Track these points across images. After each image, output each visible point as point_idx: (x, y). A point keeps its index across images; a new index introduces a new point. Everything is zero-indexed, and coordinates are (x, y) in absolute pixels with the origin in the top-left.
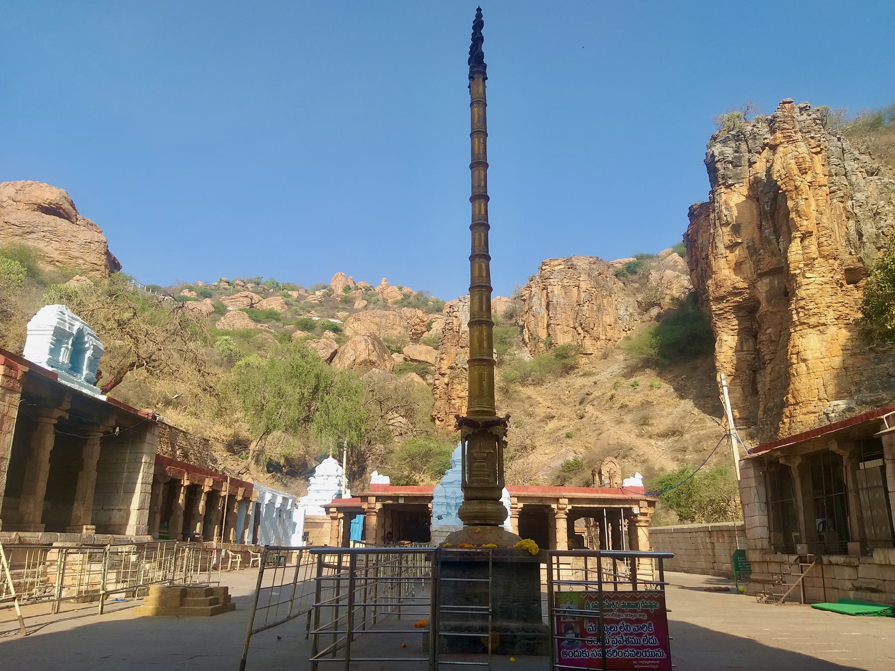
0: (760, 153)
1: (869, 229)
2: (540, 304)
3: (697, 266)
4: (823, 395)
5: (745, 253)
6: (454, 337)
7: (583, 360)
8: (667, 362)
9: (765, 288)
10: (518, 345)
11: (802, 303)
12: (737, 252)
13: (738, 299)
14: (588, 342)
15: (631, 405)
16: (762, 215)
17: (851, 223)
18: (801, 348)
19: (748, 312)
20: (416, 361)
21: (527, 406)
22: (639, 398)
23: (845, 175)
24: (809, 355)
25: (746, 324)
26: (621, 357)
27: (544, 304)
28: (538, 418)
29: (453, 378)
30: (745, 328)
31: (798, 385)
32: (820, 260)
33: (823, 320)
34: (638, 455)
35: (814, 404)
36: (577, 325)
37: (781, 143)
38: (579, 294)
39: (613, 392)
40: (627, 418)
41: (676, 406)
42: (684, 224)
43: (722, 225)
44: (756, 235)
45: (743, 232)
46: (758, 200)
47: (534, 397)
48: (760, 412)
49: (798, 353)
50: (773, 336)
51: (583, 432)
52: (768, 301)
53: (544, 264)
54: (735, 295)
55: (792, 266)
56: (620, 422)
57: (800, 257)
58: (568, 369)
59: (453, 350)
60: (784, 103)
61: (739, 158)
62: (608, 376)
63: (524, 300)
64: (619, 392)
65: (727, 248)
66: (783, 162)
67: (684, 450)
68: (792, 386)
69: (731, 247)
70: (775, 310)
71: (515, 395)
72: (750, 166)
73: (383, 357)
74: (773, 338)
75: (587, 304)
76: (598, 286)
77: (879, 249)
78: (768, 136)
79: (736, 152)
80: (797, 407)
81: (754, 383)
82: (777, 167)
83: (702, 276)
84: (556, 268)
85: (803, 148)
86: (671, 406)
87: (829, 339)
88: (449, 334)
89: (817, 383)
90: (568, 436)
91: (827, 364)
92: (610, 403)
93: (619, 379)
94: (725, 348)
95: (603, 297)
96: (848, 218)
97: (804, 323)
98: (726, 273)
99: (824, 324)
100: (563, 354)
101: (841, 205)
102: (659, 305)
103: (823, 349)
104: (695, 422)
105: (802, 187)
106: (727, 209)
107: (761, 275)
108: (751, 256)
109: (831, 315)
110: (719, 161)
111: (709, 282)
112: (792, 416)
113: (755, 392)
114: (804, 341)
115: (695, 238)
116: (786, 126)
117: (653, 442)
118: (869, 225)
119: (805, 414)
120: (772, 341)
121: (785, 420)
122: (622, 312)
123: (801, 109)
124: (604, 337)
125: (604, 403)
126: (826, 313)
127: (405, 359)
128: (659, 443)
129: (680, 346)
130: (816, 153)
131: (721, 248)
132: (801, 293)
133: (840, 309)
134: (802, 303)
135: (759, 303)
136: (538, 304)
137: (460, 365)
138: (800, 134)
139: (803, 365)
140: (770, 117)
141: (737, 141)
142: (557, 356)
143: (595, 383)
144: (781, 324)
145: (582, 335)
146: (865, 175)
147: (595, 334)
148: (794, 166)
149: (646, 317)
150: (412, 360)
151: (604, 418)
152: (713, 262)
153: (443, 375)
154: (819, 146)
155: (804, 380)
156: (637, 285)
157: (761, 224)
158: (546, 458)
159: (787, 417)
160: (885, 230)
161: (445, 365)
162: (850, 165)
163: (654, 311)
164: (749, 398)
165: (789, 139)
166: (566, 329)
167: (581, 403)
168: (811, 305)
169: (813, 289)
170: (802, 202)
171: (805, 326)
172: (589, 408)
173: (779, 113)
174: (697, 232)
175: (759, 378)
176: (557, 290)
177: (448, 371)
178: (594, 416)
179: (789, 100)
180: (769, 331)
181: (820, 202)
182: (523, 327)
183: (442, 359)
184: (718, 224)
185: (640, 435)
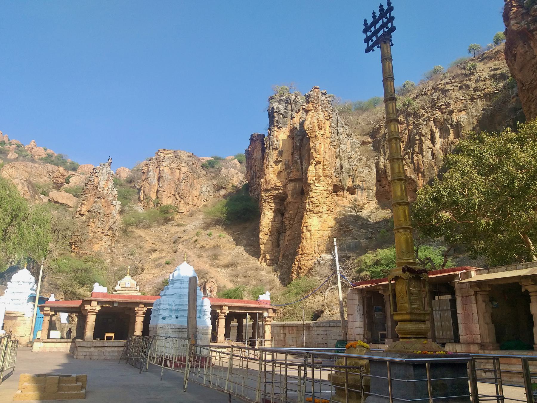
0: (297, 113)
1: (346, 165)
2: (154, 177)
3: (251, 169)
4: (317, 251)
5: (284, 167)
6: (94, 190)
7: (178, 216)
8: (229, 223)
10: (135, 201)
11: (312, 199)
12: (279, 166)
13: (276, 192)
14: (181, 205)
15: (207, 246)
16: (294, 148)
17: (338, 160)
18: (309, 224)
19: (280, 200)
20: (58, 203)
21: (138, 241)
22: (212, 243)
23: (337, 134)
24: (312, 228)
25: (278, 207)
26: (201, 217)
27: (156, 177)
28: (145, 250)
29: (89, 218)
32: (323, 177)
33: (320, 211)
34: (210, 277)
35: (312, 255)
36: (176, 193)
37: (311, 110)
38: (180, 174)
39: (196, 237)
40: (205, 254)
41: (234, 249)
42: (247, 144)
43: (273, 149)
44: (290, 158)
45: (284, 155)
46: (293, 139)
47: (144, 236)
48: (280, 257)
51: (176, 261)
52: (292, 196)
53: (159, 151)
54: (275, 189)
56: (200, 256)
57: (314, 174)
58: (167, 221)
59: (92, 199)
60: (315, 88)
61: (287, 113)
62: (193, 227)
63: (143, 173)
64: (200, 238)
65: (274, 162)
66: (311, 120)
67: (237, 276)
68: (302, 244)
69: (277, 162)
70: (295, 201)
71: (131, 233)
72: (291, 119)
73: (34, 197)
75: (184, 181)
76: (192, 171)
77: (349, 176)
78: (305, 104)
79: (285, 109)
80: (303, 256)
81: (278, 240)
82: (307, 123)
83: (253, 175)
84: (167, 156)
85: (321, 115)
86: (231, 249)
88: (90, 188)
90: (167, 263)
92: (194, 244)
93: (200, 230)
95: (194, 179)
96: (336, 157)
97: (312, 211)
98: (272, 176)
99: (322, 213)
100: (165, 211)
101: (334, 150)
102: (226, 188)
103: (319, 226)
104: (244, 260)
105: (318, 136)
106: (277, 140)
107: (290, 181)
108: (286, 169)
109: (325, 208)
111: (262, 180)
112: (300, 261)
113: (278, 245)
114: (311, 220)
116: (315, 101)
117: (219, 270)
118: (346, 163)
121: (296, 263)
122: (204, 189)
123: (323, 94)
124: (192, 203)
125: (190, 244)
127: (50, 200)
128: (223, 271)
129: (239, 214)
130: (327, 120)
131: (271, 163)
132: (312, 194)
133: (330, 205)
134: (312, 199)
135: (287, 196)
136: (153, 176)
137: (96, 210)
138: (321, 107)
139: (309, 233)
140: (307, 94)
141: (286, 103)
142: (161, 211)
143: (184, 231)
144: (298, 209)
145: (179, 200)
146: (346, 136)
147: (187, 201)
148: (316, 124)
149: (217, 195)
150: (55, 202)
151: (190, 253)
152: (266, 169)
153: (82, 215)
154: (329, 116)
156: (213, 175)
157: (293, 153)
158: (152, 276)
159: (297, 261)
160: (354, 167)
161: (84, 209)
162: (341, 130)
163: (223, 192)
164: (275, 248)
166: (169, 195)
167: (174, 243)
168: (316, 202)
169: (318, 193)
170: (318, 145)
171: (312, 212)
172: (180, 246)
173: (312, 93)
174: (254, 150)
175: (281, 238)
176: (166, 170)
177: (86, 213)
178: (184, 252)
179: (318, 87)
180: (290, 212)
181: (326, 146)
182: (139, 190)
183: (83, 204)
185: (212, 265)
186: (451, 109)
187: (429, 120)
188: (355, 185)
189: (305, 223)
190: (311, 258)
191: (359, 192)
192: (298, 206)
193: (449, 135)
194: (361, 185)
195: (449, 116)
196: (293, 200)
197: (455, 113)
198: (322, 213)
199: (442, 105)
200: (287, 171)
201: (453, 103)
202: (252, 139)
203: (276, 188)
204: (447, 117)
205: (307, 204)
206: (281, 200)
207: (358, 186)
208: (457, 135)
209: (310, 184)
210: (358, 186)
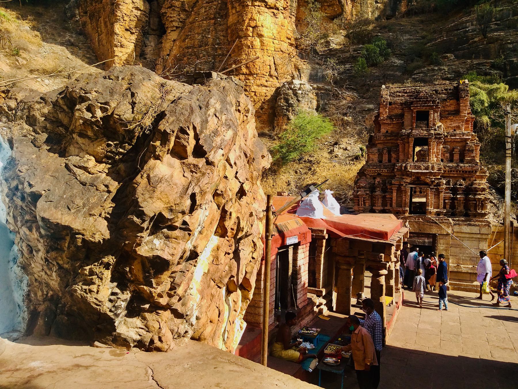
4: (273, 73)
18: (259, 24)
24: (265, 32)
49: (254, 28)
80: (251, 78)
87: (280, 24)
89: (269, 60)
91: (277, 46)
99: (277, 9)
103: (275, 32)
114: (262, 18)
119: (258, 86)
139: (258, 40)
171: (263, 4)
189: (252, 19)
190: (263, 81)
198: (277, 9)
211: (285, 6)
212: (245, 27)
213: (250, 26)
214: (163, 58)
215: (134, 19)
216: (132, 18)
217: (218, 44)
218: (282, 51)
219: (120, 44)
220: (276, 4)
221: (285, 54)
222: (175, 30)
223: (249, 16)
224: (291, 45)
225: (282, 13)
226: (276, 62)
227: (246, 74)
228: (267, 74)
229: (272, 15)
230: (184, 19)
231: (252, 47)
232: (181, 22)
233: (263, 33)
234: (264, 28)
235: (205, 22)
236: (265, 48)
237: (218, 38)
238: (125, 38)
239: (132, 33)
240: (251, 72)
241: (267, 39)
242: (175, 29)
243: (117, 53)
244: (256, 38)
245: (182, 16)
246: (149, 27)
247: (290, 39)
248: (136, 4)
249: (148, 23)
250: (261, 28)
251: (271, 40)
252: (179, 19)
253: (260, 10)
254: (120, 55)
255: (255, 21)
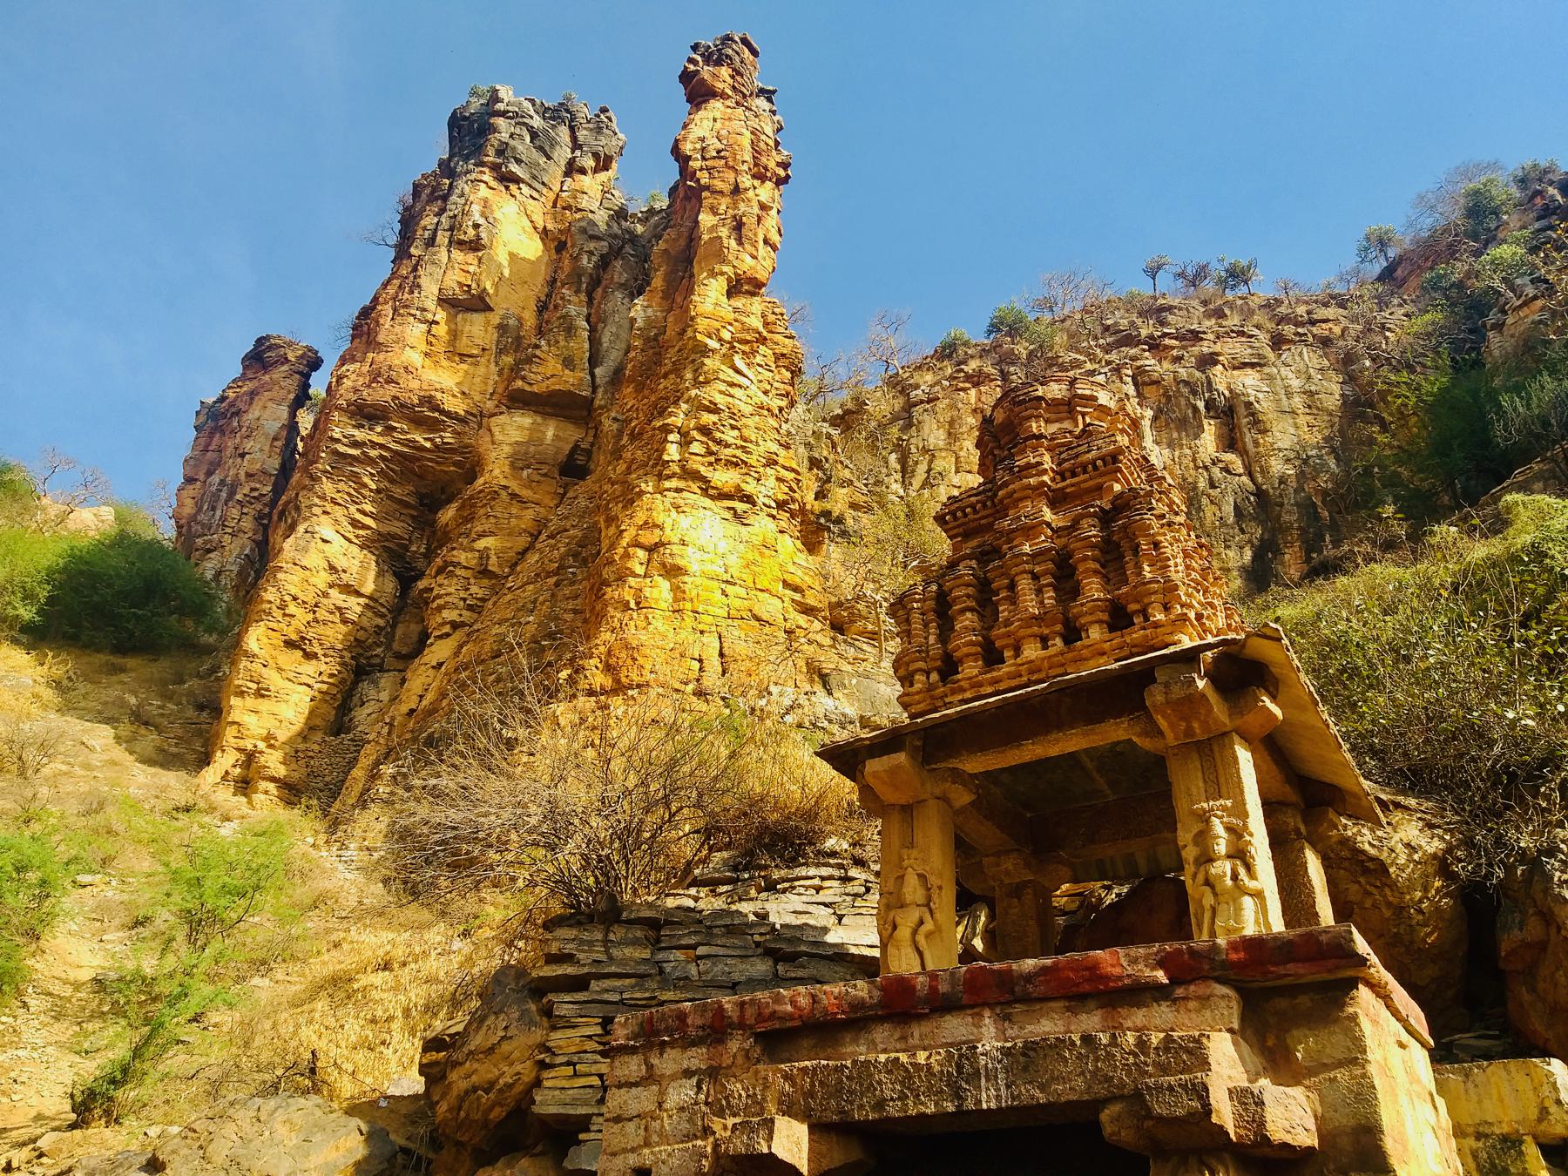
3: (209, 473)
9: (516, 436)
11: (708, 418)
18: (669, 535)
24: (689, 559)
25: (397, 527)
30: (391, 536)
31: (633, 634)
33: (751, 487)
44: (530, 318)
46: (561, 247)
49: (651, 549)
50: (493, 560)
52: (512, 465)
54: (419, 422)
55: (702, 324)
61: (553, 143)
65: (443, 301)
68: (606, 636)
70: (525, 493)
74: (493, 565)
83: (216, 495)
87: (757, 541)
91: (737, 603)
94: (314, 559)
97: (696, 476)
99: (749, 499)
103: (734, 563)
106: (483, 214)
107: (518, 400)
110: (503, 114)
115: (242, 406)
120: (484, 573)
126: (761, 470)
134: (708, 418)
139: (664, 585)
144: (535, 537)
155: (659, 624)
165: (742, 98)
168: (730, 436)
171: (694, 487)
174: (253, 394)
180: (482, 544)
184: (442, 238)
186: (1205, 349)
187: (1117, 370)
188: (826, 514)
191: (834, 551)
192: (541, 524)
193: (1197, 436)
194: (850, 522)
195: (1198, 374)
196: (514, 486)
197: (1219, 367)
199: (1165, 335)
200: (508, 360)
201: (1211, 337)
202: (260, 357)
203: (426, 413)
204: (1190, 375)
205: (673, 437)
206: (421, 497)
207: (840, 520)
208: (1230, 442)
209: (705, 351)
210: (840, 520)
211: (781, 497)
212: (620, 551)
213: (639, 545)
214: (391, 725)
215: (331, 617)
216: (322, 614)
217: (551, 636)
218: (758, 619)
219: (254, 686)
220: (744, 486)
221: (767, 629)
222: (448, 635)
223: (640, 517)
224: (807, 610)
225: (774, 517)
226: (726, 651)
227: (604, 692)
228: (690, 688)
229: (728, 515)
230: (483, 600)
231: (638, 604)
232: (470, 608)
233: (680, 562)
234: (689, 550)
235: (531, 587)
236: (688, 606)
237: (556, 618)
238: (280, 669)
239: (310, 656)
240: (617, 681)
241: (698, 581)
242: (447, 629)
243: (235, 716)
244: (657, 578)
245: (474, 589)
246: (389, 647)
247: (796, 589)
248: (343, 575)
249: (385, 634)
250: (676, 549)
251: (716, 584)
252: (464, 600)
253: (681, 502)
254: (250, 720)
255: (657, 531)
